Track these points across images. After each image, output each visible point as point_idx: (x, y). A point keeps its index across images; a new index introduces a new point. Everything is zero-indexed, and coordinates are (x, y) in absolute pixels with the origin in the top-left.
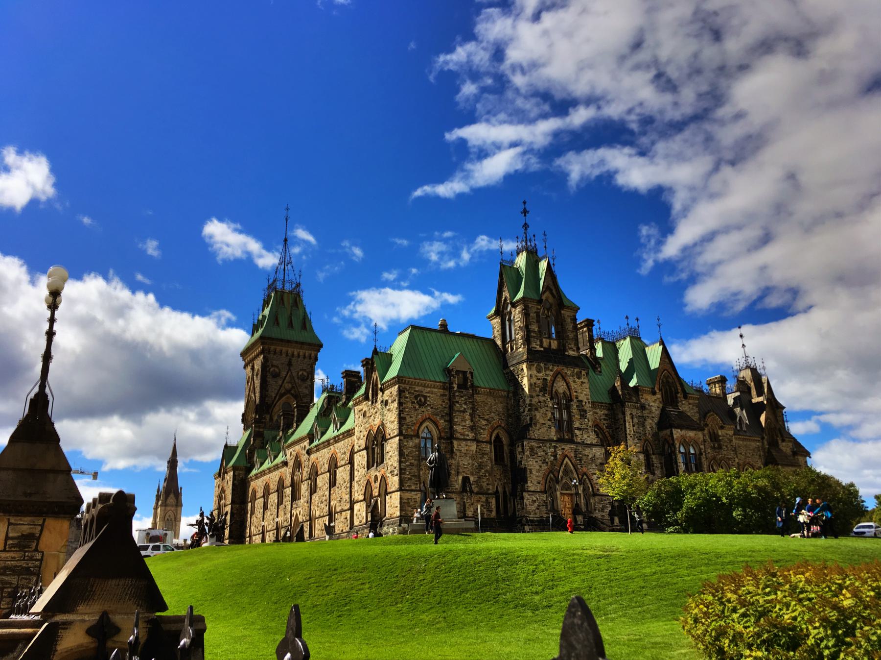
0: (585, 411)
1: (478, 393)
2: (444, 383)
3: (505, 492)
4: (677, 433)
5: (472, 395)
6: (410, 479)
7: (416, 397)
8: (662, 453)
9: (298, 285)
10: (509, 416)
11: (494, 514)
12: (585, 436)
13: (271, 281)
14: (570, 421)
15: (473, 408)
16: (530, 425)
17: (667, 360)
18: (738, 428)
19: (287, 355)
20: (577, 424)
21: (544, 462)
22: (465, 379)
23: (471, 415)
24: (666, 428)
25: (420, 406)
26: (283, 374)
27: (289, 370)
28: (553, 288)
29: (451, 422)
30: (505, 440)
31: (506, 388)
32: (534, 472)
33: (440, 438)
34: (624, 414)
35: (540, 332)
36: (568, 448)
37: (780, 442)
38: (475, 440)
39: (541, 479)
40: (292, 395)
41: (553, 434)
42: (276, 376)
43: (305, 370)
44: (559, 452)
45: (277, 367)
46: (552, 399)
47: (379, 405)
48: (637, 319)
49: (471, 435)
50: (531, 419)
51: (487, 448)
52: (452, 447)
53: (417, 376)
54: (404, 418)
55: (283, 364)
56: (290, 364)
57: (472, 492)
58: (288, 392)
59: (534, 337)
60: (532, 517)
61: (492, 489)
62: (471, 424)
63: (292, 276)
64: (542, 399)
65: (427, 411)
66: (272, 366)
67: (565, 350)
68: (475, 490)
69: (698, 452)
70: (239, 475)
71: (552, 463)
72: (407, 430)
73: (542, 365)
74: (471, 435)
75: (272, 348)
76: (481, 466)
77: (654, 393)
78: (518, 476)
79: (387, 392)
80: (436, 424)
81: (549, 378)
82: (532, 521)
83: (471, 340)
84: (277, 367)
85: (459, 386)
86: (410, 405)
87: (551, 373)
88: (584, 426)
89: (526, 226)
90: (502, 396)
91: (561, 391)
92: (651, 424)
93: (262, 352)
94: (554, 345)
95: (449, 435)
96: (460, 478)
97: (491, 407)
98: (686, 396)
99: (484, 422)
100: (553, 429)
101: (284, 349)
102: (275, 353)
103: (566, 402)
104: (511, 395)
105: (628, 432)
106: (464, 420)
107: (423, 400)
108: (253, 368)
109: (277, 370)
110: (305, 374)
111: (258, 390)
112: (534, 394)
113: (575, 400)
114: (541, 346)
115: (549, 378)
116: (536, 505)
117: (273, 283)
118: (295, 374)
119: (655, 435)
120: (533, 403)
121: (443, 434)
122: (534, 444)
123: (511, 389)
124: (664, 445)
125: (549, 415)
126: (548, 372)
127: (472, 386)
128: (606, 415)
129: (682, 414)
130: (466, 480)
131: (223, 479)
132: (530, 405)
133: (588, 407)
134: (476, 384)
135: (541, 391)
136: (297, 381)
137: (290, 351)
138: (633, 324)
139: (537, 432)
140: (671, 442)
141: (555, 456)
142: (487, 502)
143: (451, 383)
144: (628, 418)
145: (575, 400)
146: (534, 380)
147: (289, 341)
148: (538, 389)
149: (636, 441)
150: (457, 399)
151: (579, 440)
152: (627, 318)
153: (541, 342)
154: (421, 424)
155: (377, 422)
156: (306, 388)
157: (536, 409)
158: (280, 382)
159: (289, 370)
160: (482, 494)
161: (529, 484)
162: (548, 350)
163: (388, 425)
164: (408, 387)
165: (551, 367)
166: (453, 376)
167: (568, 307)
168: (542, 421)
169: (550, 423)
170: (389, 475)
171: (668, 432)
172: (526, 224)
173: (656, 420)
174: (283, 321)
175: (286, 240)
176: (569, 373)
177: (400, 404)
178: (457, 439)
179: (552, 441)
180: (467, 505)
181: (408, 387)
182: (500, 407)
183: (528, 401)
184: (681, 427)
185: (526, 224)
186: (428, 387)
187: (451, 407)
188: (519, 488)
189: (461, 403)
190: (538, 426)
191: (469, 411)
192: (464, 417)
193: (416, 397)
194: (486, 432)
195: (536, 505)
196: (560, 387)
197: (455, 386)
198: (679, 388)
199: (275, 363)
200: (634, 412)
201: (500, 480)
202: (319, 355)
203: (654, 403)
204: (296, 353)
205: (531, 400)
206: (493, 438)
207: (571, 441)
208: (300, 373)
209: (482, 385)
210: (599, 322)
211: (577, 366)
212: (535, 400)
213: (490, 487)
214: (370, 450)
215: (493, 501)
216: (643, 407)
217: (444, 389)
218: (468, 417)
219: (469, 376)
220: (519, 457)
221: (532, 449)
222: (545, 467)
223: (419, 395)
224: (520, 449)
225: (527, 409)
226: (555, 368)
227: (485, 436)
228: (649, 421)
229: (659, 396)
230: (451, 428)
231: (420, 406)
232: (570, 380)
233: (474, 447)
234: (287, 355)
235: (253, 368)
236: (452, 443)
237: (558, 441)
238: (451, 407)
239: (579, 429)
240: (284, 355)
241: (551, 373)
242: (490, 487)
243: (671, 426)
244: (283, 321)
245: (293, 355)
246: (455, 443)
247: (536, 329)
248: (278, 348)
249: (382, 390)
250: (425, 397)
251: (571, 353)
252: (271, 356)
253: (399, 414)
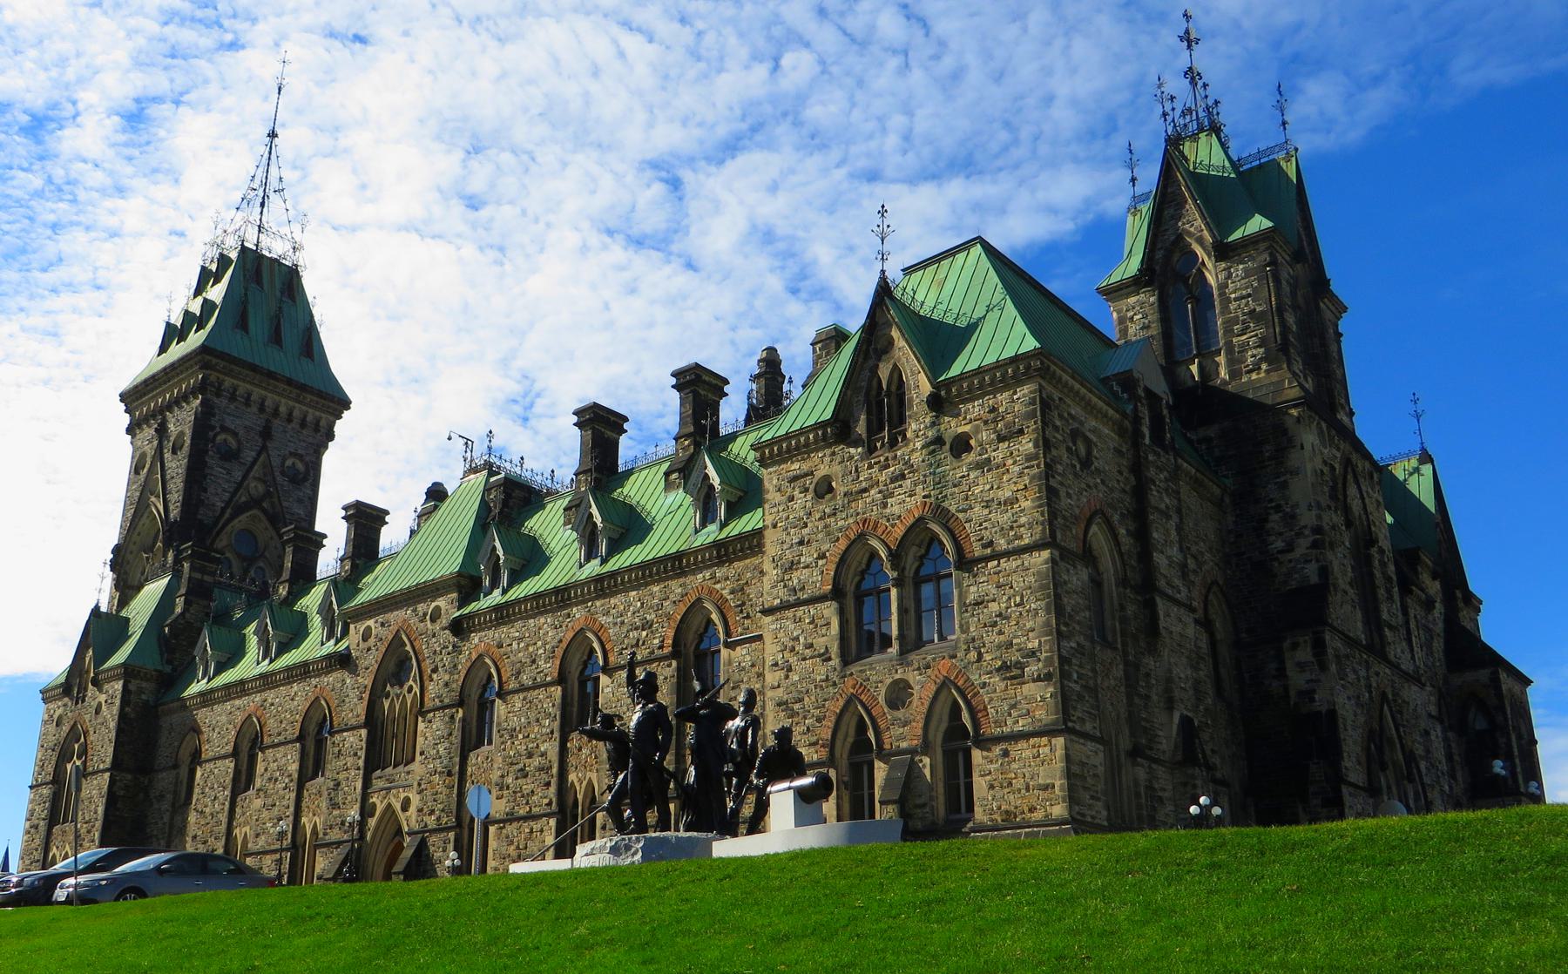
6: (1081, 697)
19: (262, 409)
26: (248, 455)
27: (264, 448)
33: (1123, 582)
40: (264, 511)
43: (300, 457)
45: (235, 434)
56: (266, 433)
58: (255, 503)
66: (224, 429)
70: (141, 691)
75: (228, 382)
84: (235, 434)
101: (257, 393)
102: (233, 398)
108: (162, 431)
110: (300, 466)
118: (276, 462)
132: (1318, 530)
136: (279, 479)
155: (905, 505)
156: (300, 501)
158: (238, 475)
159: (264, 448)
187: (1140, 492)
191: (1175, 518)
199: (229, 423)
202: (339, 426)
204: (282, 409)
205: (1319, 517)
208: (289, 463)
234: (262, 409)
235: (162, 431)
238: (1140, 492)
240: (254, 409)
245: (276, 413)
248: (243, 387)
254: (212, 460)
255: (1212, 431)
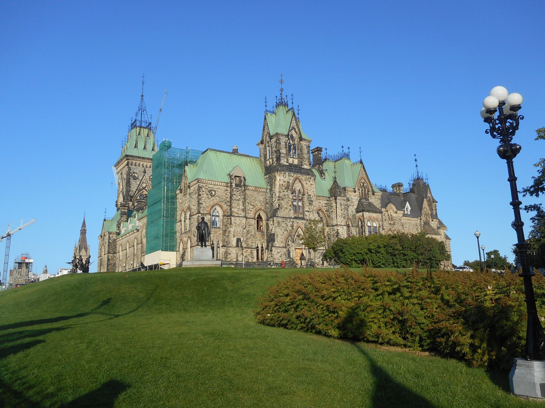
0: (312, 201)
1: (249, 190)
2: (227, 183)
3: (262, 247)
4: (366, 214)
5: (245, 190)
7: (209, 191)
8: (358, 226)
9: (150, 124)
10: (267, 203)
11: (255, 260)
12: (311, 216)
13: (133, 122)
14: (303, 207)
15: (245, 199)
16: (278, 209)
17: (364, 172)
18: (406, 213)
20: (306, 209)
21: (286, 230)
22: (241, 181)
23: (243, 202)
24: (360, 212)
25: (212, 196)
26: (140, 178)
28: (296, 127)
29: (231, 206)
30: (264, 217)
31: (265, 187)
32: (279, 236)
33: (224, 216)
34: (336, 203)
35: (287, 154)
36: (300, 222)
37: (431, 221)
38: (245, 217)
39: (283, 240)
40: (146, 190)
41: (292, 214)
42: (135, 178)
44: (295, 225)
46: (292, 193)
47: (188, 196)
48: (349, 148)
49: (243, 214)
50: (279, 205)
51: (254, 222)
52: (231, 221)
53: (210, 179)
54: (202, 204)
55: (140, 171)
56: (145, 172)
57: (242, 247)
59: (283, 157)
60: (276, 261)
61: (254, 246)
62: (243, 207)
63: (146, 119)
64: (286, 193)
65: (216, 200)
66: (134, 173)
67: (302, 165)
68: (244, 245)
69: (378, 226)
71: (291, 231)
72: (203, 210)
73: (287, 173)
74: (243, 214)
75: (134, 162)
76: (248, 232)
77: (355, 192)
78: (271, 239)
79: (192, 188)
80: (221, 207)
81: (291, 182)
82: (277, 264)
83: (246, 158)
85: (236, 185)
86: (205, 195)
87: (293, 178)
88: (311, 210)
89: (282, 90)
90: (263, 192)
91: (298, 189)
92: (352, 209)
93: (128, 164)
94: (296, 162)
95: (229, 214)
96: (235, 239)
97: (256, 198)
98: (373, 194)
99: (252, 207)
100: (292, 211)
103: (300, 196)
104: (268, 191)
105: (338, 214)
106: (238, 204)
107: (213, 193)
108: (121, 174)
109: (136, 175)
111: (125, 186)
112: (281, 191)
113: (306, 195)
114: (287, 162)
115: (291, 182)
116: (279, 254)
117: (134, 123)
119: (354, 216)
120: (281, 196)
121: (225, 213)
122: (280, 219)
123: (269, 187)
124: (358, 222)
125: (290, 203)
126: (290, 178)
127: (244, 185)
128: (326, 204)
129: (370, 204)
130: (238, 240)
131: (103, 240)
133: (314, 199)
134: (247, 184)
135: (286, 189)
137: (145, 164)
138: (346, 151)
139: (281, 213)
140: (362, 220)
141: (293, 227)
142: (251, 252)
143: (231, 183)
144: (338, 206)
145: (306, 195)
146: (282, 182)
147: (143, 158)
148: (284, 188)
149: (342, 219)
150: (235, 193)
151: (307, 218)
152: (343, 147)
153: (287, 160)
154: (212, 207)
155: (187, 205)
157: (282, 199)
160: (248, 248)
161: (276, 242)
162: (291, 165)
163: (192, 207)
164: (204, 185)
165: (292, 175)
166: (232, 179)
167: (305, 140)
168: (285, 206)
169: (290, 208)
170: (192, 237)
171: (361, 214)
172: (282, 89)
173: (355, 207)
174: (141, 145)
175: (142, 96)
176: (303, 178)
177: (199, 195)
178: (233, 216)
179: (291, 218)
180: (239, 254)
181: (204, 185)
182: (261, 198)
183: (277, 195)
184: (369, 211)
185: (282, 89)
186: (217, 185)
188: (270, 245)
189: (237, 195)
190: (283, 209)
192: (238, 203)
193: (209, 191)
194: (252, 212)
195: (279, 254)
196: (298, 186)
197: (234, 185)
198: (370, 189)
200: (342, 202)
201: (260, 240)
203: (355, 198)
204: (148, 165)
206: (256, 216)
207: (303, 219)
209: (251, 185)
210: (326, 149)
211: (309, 174)
212: (282, 194)
213: (254, 244)
214: (183, 222)
215: (255, 252)
216: (348, 200)
217: (227, 186)
218: (241, 203)
219: (242, 179)
220: (271, 227)
221: (278, 222)
222: (286, 233)
223: (211, 190)
224: (272, 223)
225: (277, 199)
226: (295, 175)
227: (251, 214)
228: (351, 208)
229: (358, 193)
230: (231, 209)
231: (212, 196)
232: (304, 183)
233: (244, 220)
235: (121, 174)
236: (231, 218)
237: (295, 218)
238: (231, 197)
239: (308, 211)
240: (141, 166)
241: (293, 178)
242: (254, 244)
243: (363, 211)
244: (141, 145)
246: (232, 218)
247: (285, 152)
249: (189, 187)
250: (215, 191)
251: (305, 167)
252: (133, 166)
253: (199, 201)
254: (132, 180)
255: (267, 176)
